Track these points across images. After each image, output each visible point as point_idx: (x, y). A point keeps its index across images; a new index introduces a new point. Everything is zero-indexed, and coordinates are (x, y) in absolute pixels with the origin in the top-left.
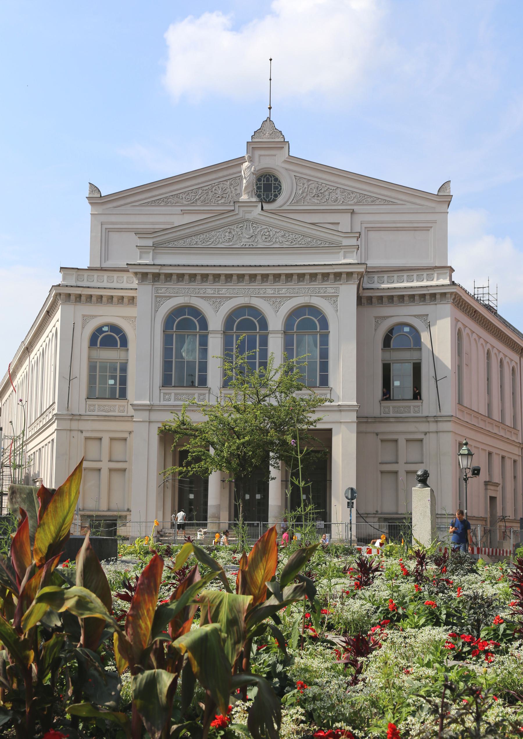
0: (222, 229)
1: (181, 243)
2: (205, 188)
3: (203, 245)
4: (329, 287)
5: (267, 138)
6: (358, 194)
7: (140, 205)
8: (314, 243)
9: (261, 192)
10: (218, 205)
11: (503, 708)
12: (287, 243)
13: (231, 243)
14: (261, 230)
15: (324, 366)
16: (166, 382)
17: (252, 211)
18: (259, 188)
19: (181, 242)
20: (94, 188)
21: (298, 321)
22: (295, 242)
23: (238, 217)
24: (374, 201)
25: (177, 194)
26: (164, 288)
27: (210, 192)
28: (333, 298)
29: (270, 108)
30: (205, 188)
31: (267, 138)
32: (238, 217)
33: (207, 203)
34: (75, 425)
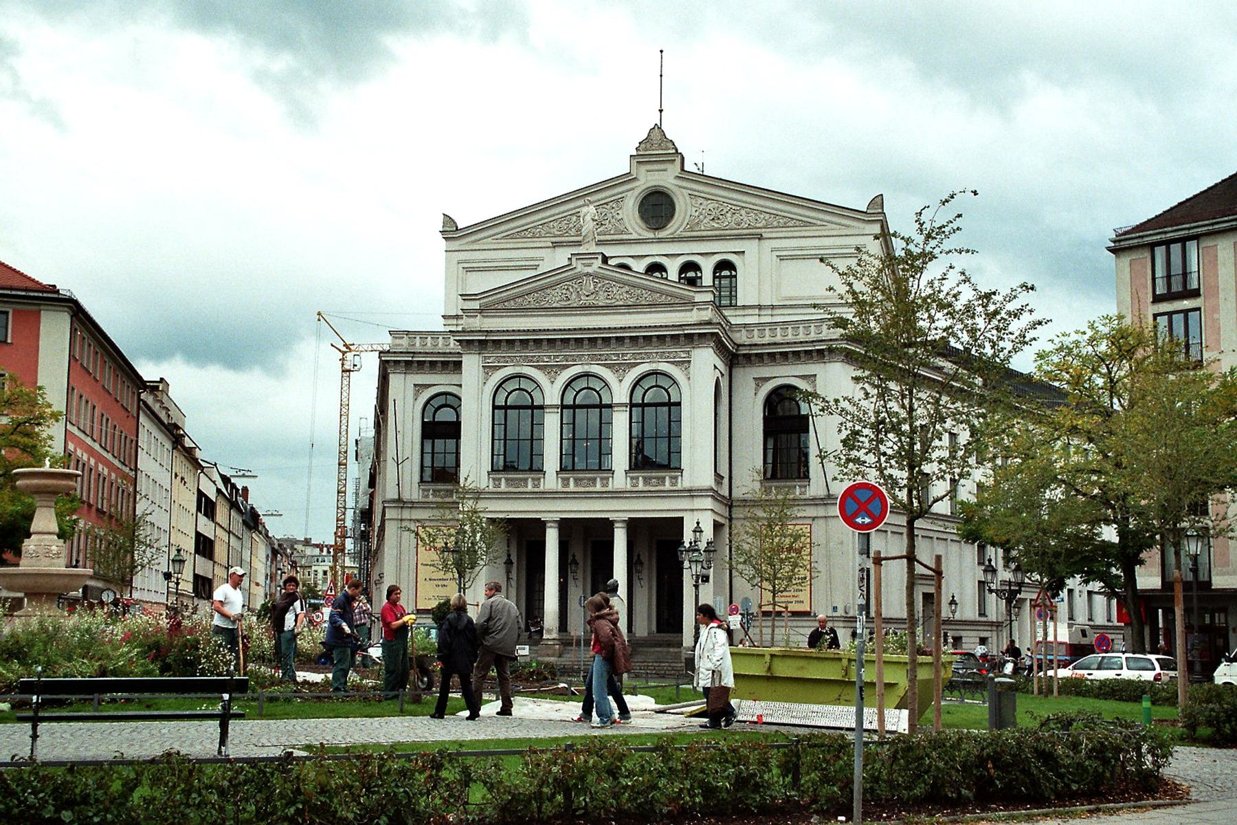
4: (680, 352)
5: (656, 148)
7: (503, 238)
11: (591, 778)
20: (448, 220)
24: (788, 223)
26: (493, 357)
28: (685, 364)
29: (661, 111)
31: (656, 148)
34: (406, 514)
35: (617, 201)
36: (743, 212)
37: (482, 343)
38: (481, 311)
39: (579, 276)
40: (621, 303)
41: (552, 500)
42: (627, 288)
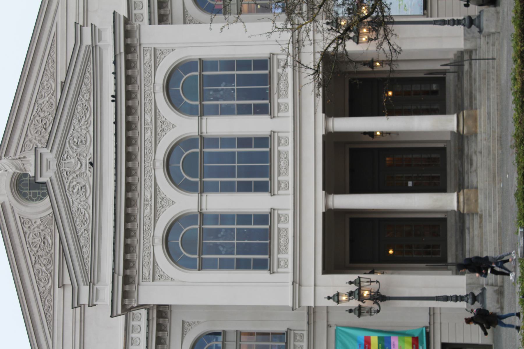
0: (70, 198)
1: (87, 251)
2: (33, 259)
3: (89, 221)
6: (44, 77)
8: (88, 81)
9: (39, 193)
10: (54, 243)
12: (88, 116)
13: (87, 186)
14: (71, 148)
15: (244, 64)
16: (262, 265)
17: (47, 160)
18: (35, 195)
19: (84, 250)
21: (185, 100)
22: (87, 106)
23: (54, 178)
25: (40, 293)
26: (143, 269)
27: (39, 254)
30: (33, 259)
32: (54, 178)
33: (51, 257)
35: (23, 223)
36: (40, 101)
37: (127, 280)
38: (91, 283)
39: (59, 173)
40: (91, 129)
41: (299, 202)
42: (75, 121)
